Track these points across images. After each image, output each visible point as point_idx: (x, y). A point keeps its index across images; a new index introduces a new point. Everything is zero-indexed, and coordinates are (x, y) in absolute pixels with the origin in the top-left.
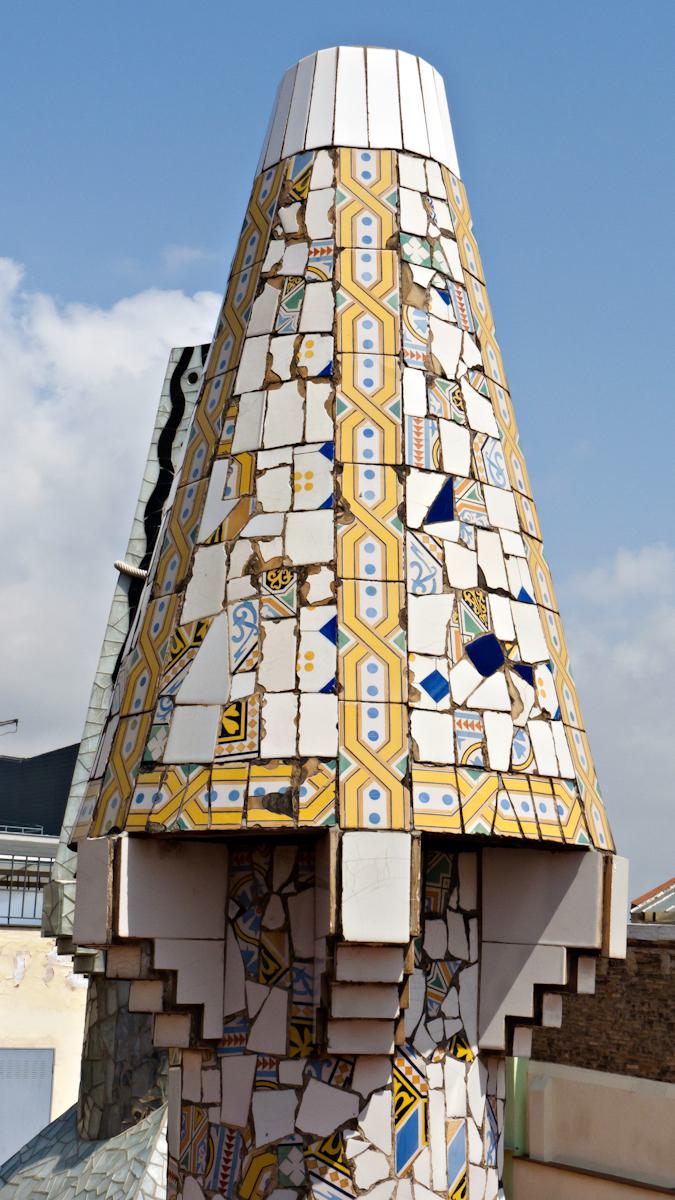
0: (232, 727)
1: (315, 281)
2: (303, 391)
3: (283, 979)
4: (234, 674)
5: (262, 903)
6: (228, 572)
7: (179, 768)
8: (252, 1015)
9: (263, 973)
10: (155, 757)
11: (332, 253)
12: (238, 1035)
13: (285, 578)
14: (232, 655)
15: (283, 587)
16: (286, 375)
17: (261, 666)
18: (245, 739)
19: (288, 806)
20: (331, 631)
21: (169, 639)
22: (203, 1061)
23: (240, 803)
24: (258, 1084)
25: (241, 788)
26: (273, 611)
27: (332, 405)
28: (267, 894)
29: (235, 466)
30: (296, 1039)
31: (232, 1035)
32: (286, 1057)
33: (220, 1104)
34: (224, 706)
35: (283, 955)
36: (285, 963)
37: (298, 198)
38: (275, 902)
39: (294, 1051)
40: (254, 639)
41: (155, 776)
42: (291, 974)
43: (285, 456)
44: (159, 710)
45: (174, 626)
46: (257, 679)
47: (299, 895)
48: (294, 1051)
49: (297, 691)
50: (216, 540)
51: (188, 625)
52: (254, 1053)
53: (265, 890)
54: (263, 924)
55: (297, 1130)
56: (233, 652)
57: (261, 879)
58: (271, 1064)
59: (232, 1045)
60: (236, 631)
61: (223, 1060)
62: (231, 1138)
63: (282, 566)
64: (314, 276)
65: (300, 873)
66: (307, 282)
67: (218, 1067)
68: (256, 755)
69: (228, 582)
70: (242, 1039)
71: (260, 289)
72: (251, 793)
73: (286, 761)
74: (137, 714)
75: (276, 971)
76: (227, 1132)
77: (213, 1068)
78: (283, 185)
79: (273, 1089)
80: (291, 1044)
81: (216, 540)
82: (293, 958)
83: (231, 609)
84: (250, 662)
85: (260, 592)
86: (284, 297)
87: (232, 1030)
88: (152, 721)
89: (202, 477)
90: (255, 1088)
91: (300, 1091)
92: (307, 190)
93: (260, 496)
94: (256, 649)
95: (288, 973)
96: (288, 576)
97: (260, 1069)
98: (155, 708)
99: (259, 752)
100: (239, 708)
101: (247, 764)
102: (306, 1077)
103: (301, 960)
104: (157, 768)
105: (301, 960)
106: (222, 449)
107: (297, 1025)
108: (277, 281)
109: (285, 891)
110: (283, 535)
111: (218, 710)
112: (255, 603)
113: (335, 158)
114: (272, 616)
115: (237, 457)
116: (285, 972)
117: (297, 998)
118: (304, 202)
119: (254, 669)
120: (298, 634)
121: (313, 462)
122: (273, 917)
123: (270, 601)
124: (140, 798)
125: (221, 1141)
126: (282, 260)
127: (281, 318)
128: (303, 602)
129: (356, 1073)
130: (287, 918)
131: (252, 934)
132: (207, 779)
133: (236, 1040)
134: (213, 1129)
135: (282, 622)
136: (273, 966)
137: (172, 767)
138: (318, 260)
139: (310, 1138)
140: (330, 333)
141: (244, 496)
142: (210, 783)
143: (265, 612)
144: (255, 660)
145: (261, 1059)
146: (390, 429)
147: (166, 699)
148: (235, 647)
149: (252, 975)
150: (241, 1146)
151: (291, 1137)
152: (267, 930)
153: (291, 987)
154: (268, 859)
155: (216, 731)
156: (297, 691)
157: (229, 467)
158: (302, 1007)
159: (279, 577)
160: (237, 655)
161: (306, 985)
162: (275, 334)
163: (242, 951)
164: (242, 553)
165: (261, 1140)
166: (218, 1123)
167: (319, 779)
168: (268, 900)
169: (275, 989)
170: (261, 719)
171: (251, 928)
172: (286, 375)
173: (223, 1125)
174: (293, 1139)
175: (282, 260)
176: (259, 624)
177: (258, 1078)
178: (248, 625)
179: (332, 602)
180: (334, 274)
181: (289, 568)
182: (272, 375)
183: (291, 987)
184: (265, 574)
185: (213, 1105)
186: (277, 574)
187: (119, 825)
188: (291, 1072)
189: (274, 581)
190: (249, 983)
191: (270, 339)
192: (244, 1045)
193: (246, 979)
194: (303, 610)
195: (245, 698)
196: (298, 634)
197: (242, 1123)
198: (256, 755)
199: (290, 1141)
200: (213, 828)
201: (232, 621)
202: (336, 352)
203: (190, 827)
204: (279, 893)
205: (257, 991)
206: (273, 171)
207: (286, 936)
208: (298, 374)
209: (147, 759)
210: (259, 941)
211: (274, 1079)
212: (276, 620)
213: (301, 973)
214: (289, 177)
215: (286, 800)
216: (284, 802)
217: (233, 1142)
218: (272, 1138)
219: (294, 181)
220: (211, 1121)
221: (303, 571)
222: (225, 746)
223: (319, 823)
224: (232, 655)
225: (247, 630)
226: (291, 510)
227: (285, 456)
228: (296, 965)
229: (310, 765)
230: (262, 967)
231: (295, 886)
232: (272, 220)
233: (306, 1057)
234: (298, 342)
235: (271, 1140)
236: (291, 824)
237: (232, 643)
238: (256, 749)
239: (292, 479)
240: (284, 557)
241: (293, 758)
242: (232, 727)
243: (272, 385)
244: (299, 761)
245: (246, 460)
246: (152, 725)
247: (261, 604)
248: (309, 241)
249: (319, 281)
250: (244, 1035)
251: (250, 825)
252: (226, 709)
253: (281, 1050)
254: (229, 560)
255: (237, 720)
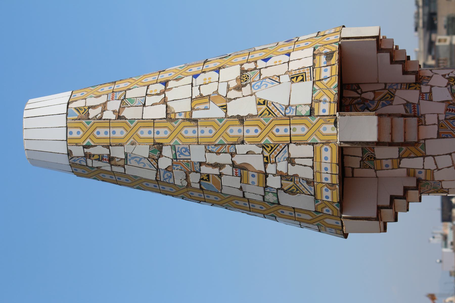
0: (300, 78)
1: (125, 96)
2: (171, 89)
3: (392, 92)
4: (280, 83)
5: (365, 100)
6: (239, 98)
7: (314, 95)
8: (405, 102)
9: (390, 98)
10: (308, 108)
11: (114, 93)
12: (412, 108)
13: (244, 76)
14: (272, 85)
15: (248, 76)
16: (163, 96)
17: (278, 75)
18: (305, 73)
19: (331, 54)
20: (266, 60)
21: (262, 119)
22: (422, 125)
23: (329, 68)
24: (430, 99)
25: (323, 69)
26: (257, 77)
27: (177, 80)
28: (361, 98)
29: (196, 108)
30: (414, 88)
31: (413, 110)
32: (420, 91)
33: (438, 114)
34: (292, 83)
35: (383, 92)
36: (386, 91)
37: (87, 110)
38: (363, 95)
39: (418, 88)
40: (268, 80)
41: (315, 106)
42: (391, 89)
43: (196, 89)
44: (290, 114)
45: (257, 118)
46: (282, 75)
47: (361, 88)
48: (418, 88)
49: (288, 62)
50: (225, 107)
51: (258, 110)
52: (419, 101)
53: (359, 99)
54: (372, 99)
55: (446, 87)
56: (272, 85)
57: (356, 101)
58: (423, 95)
59: (416, 110)
60: (263, 87)
61: (422, 113)
62: (450, 110)
63: (240, 79)
64: (123, 96)
65: (353, 88)
66: (125, 98)
67: (424, 115)
68: (311, 68)
69: (244, 96)
70: (414, 106)
71: (124, 118)
72: (326, 65)
73: (314, 58)
74: (290, 129)
75: (389, 94)
76: (448, 111)
77: (425, 117)
78: (79, 119)
79: (431, 94)
80: (415, 89)
81: (225, 107)
82: (385, 89)
83: (254, 91)
84: (276, 80)
85: (249, 83)
86: (129, 105)
87: (410, 110)
88: (294, 116)
89: (197, 126)
90: (431, 100)
91: (432, 86)
92: (85, 107)
93: (210, 93)
94: (271, 78)
95: (390, 90)
96: (244, 76)
97: (425, 99)
98: (289, 117)
99: (310, 67)
100: (293, 78)
101: (314, 70)
102: (427, 85)
103: (385, 87)
104: (313, 106)
105: (385, 87)
106: (188, 117)
107: (409, 86)
108: (121, 110)
109: (360, 92)
110: (227, 82)
111: (293, 85)
112: (253, 84)
113: (72, 102)
114: (259, 76)
115: (192, 107)
116: (391, 93)
117: (399, 88)
118: (89, 108)
119: (279, 77)
120: (266, 67)
121: (199, 80)
122: (370, 96)
123: (253, 79)
124: (324, 111)
125: (451, 114)
126: (112, 111)
127: (138, 104)
128: (255, 69)
129: (426, 76)
130: (370, 91)
131: (375, 104)
132: (319, 82)
133: (414, 108)
134: (448, 117)
135: (261, 73)
136: (387, 96)
137: (313, 99)
138: (116, 97)
139: (448, 84)
140: (148, 86)
141: (209, 100)
142: (320, 80)
143: (258, 79)
144: (275, 77)
145: (421, 99)
146: (189, 67)
147: (287, 111)
148: (269, 85)
149: (391, 103)
150: (452, 106)
151: (448, 89)
152: (374, 98)
153: (395, 89)
154: (348, 99)
155: (302, 83)
156: (288, 62)
157: (196, 110)
158: (402, 86)
159: (244, 78)
160: (272, 83)
161: (394, 85)
162: (144, 105)
163: (382, 107)
164: (233, 94)
165: (450, 98)
166: (444, 115)
167: (321, 50)
168: (363, 98)
169: (396, 94)
170: (298, 69)
171: (373, 104)
172: (163, 96)
173: (445, 113)
174: (449, 88)
175: (112, 111)
176: (261, 80)
177: (428, 99)
178: (261, 84)
179: (256, 62)
180: (124, 91)
181: (241, 76)
182: (161, 102)
183: (395, 89)
184: (242, 83)
185: (438, 118)
186: (243, 79)
187: (333, 121)
188: (425, 89)
189: (245, 79)
190: (393, 104)
191: (146, 106)
192: (416, 105)
193: (392, 105)
194: (257, 68)
195: (289, 77)
196: (266, 67)
197: (444, 105)
198: (311, 68)
199: (450, 89)
200: (337, 74)
201: (260, 89)
202: (157, 83)
203: (337, 83)
204: (361, 94)
205: (396, 101)
206: (69, 130)
207: (376, 91)
208: (163, 92)
209: (309, 114)
210: (378, 101)
211: (428, 94)
212: (260, 75)
213: (390, 87)
214: (76, 117)
215: (329, 55)
216: (329, 56)
217: (451, 109)
218: (449, 94)
219: (78, 114)
220: (444, 119)
221: (243, 71)
222: (307, 79)
223: (338, 46)
224: (272, 85)
225: (263, 83)
226: (218, 82)
227: (196, 89)
228: (387, 88)
229: (315, 52)
230: (388, 99)
231: (358, 90)
232: (93, 121)
233: (420, 85)
234: (149, 95)
235: (450, 95)
236: (337, 52)
237: (268, 87)
238: (309, 68)
239: (206, 84)
240: (237, 79)
241: (313, 57)
242: (300, 78)
243: (165, 101)
244: (314, 55)
245: (195, 102)
246: (296, 116)
247: (253, 81)
248: (108, 101)
249: (125, 95)
250: (412, 105)
251: (337, 62)
252: (293, 82)
253: (418, 92)
254: (234, 99)
255: (297, 77)
